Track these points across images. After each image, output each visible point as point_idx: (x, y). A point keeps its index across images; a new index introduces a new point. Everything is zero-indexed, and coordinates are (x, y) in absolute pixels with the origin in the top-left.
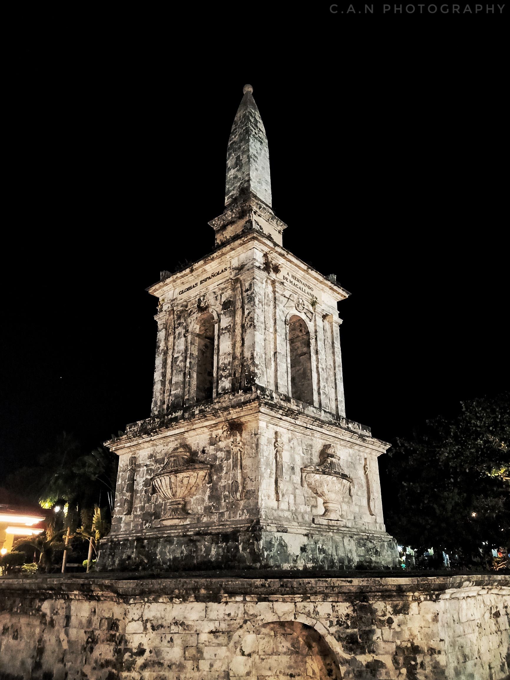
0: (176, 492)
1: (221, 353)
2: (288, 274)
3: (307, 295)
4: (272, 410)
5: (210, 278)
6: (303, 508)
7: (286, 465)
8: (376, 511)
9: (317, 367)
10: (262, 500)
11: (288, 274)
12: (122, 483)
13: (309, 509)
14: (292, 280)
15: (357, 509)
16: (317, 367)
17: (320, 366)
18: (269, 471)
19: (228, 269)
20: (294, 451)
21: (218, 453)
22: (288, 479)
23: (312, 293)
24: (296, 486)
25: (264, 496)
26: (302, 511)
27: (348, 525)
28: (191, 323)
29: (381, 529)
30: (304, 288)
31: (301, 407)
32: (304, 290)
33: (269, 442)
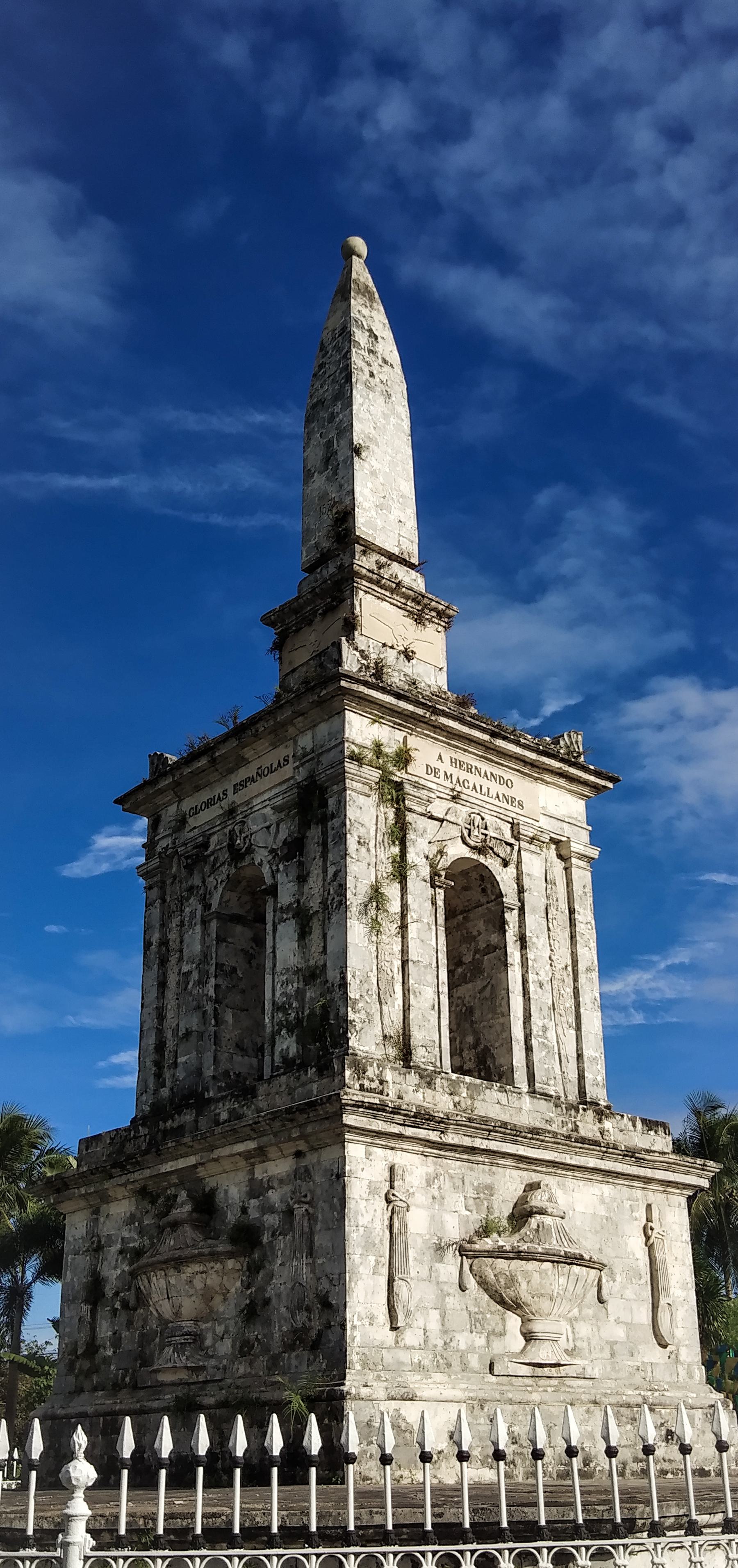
0: (180, 1306)
1: (279, 968)
2: (440, 757)
3: (496, 802)
4: (375, 1117)
5: (253, 780)
6: (463, 1340)
7: (419, 1241)
8: (679, 1333)
9: (525, 982)
10: (354, 1327)
11: (440, 757)
12: (72, 1279)
13: (481, 1341)
14: (451, 770)
15: (620, 1333)
16: (525, 982)
17: (531, 977)
18: (372, 1259)
19: (291, 759)
20: (442, 1204)
21: (266, 1217)
22: (425, 1273)
23: (509, 793)
24: (445, 1288)
25: (360, 1319)
26: (462, 1346)
27: (589, 1373)
28: (216, 888)
29: (691, 1377)
30: (486, 783)
31: (464, 1095)
32: (485, 790)
33: (373, 1190)
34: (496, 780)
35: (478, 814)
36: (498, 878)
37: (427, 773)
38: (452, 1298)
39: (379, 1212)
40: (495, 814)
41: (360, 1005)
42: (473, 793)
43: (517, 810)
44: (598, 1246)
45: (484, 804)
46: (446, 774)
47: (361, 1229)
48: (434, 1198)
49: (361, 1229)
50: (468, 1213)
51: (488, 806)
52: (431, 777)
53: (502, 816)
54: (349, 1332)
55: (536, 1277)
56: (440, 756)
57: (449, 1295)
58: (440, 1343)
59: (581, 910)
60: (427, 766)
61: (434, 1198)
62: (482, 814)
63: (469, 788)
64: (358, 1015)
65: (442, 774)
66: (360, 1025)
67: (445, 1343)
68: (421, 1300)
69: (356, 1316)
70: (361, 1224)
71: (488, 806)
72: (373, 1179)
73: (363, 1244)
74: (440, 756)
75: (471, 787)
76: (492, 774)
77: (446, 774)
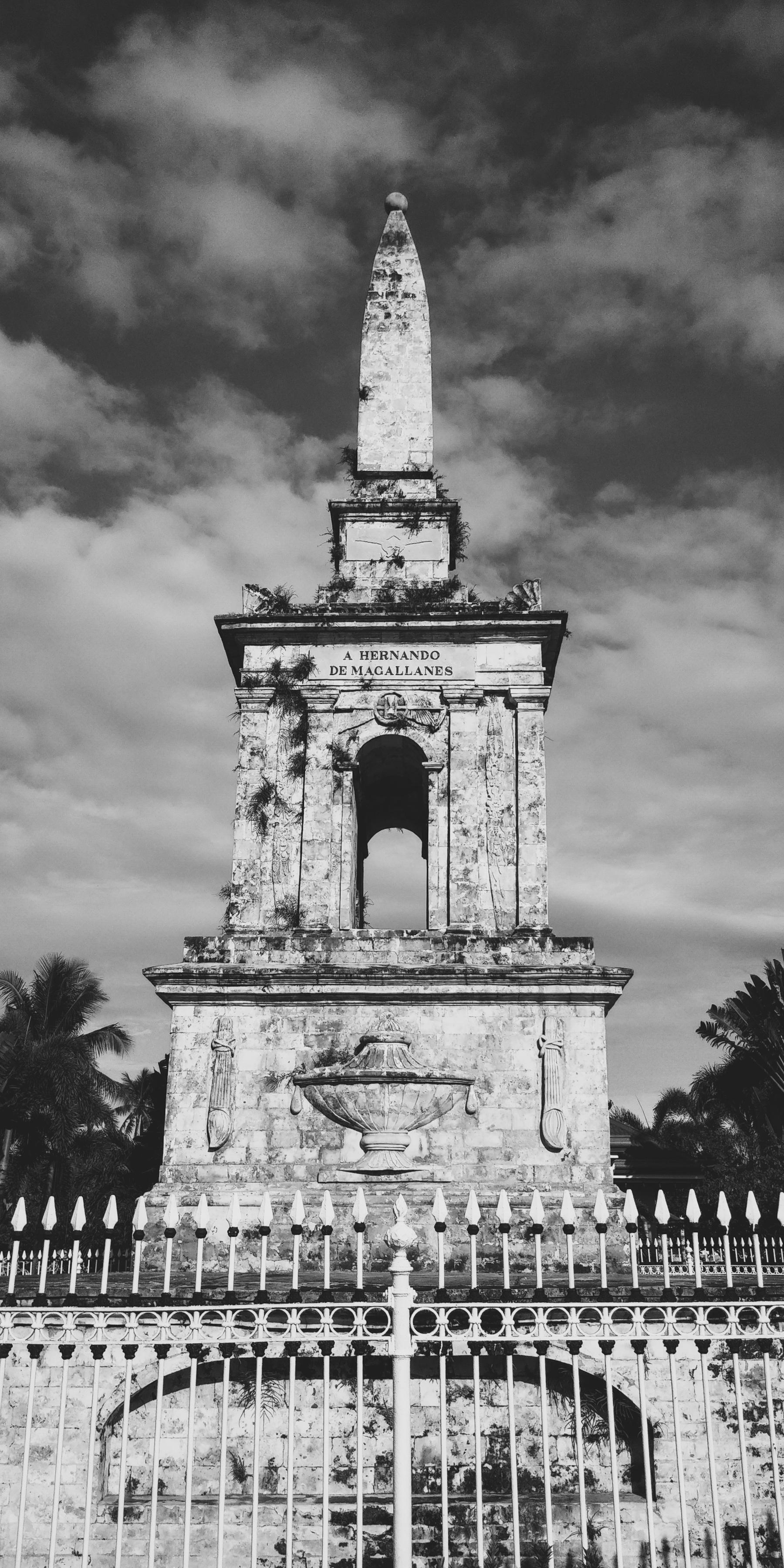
3: (418, 677)
6: (290, 1155)
7: (249, 1078)
10: (170, 1150)
11: (348, 656)
18: (193, 1096)
22: (252, 1101)
26: (290, 1159)
30: (402, 664)
31: (319, 949)
33: (199, 1041)
34: (417, 657)
35: (394, 693)
36: (422, 745)
37: (331, 674)
38: (281, 1121)
39: (204, 1057)
40: (418, 688)
41: (244, 889)
42: (389, 676)
43: (444, 677)
44: (472, 1062)
45: (403, 683)
46: (354, 668)
47: (184, 1074)
48: (268, 1040)
49: (184, 1074)
50: (308, 1049)
51: (408, 683)
52: (338, 676)
53: (426, 688)
54: (165, 1154)
55: (362, 1098)
56: (348, 654)
57: (277, 1118)
58: (264, 1158)
59: (527, 751)
60: (332, 668)
61: (268, 1040)
62: (398, 692)
63: (382, 673)
64: (241, 898)
65: (349, 670)
66: (243, 906)
67: (270, 1158)
68: (245, 1124)
69: (173, 1142)
70: (184, 1068)
71: (408, 683)
72: (200, 1032)
73: (185, 1084)
74: (348, 654)
75: (385, 670)
76: (412, 652)
77: (354, 668)
